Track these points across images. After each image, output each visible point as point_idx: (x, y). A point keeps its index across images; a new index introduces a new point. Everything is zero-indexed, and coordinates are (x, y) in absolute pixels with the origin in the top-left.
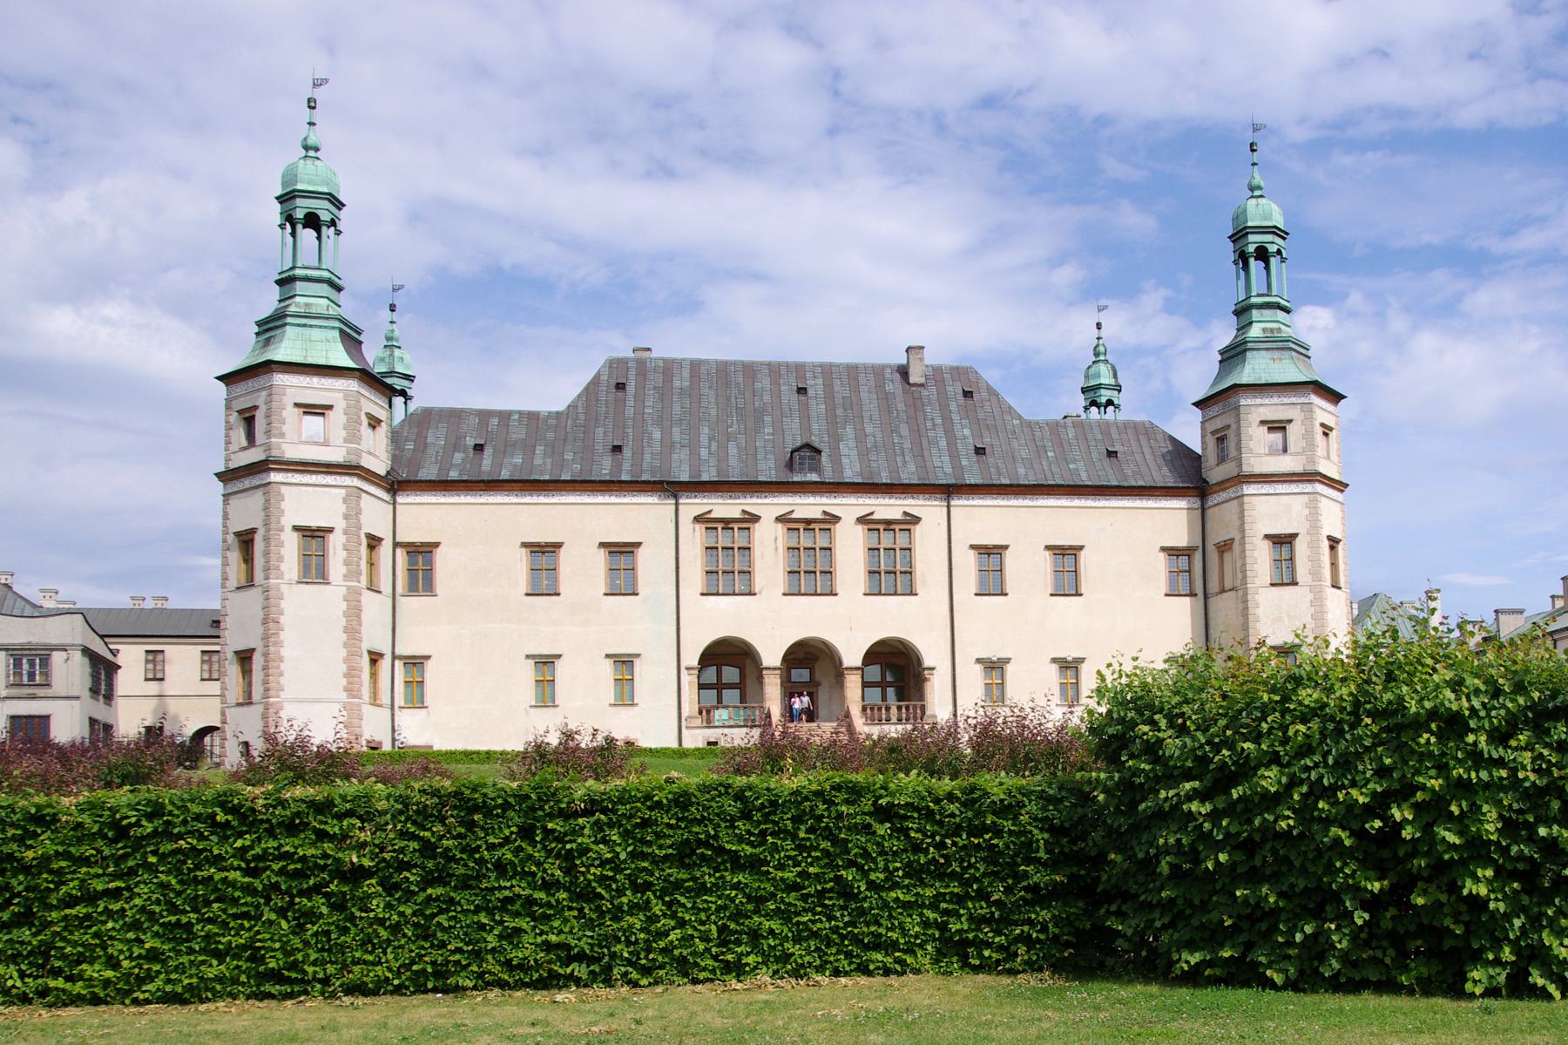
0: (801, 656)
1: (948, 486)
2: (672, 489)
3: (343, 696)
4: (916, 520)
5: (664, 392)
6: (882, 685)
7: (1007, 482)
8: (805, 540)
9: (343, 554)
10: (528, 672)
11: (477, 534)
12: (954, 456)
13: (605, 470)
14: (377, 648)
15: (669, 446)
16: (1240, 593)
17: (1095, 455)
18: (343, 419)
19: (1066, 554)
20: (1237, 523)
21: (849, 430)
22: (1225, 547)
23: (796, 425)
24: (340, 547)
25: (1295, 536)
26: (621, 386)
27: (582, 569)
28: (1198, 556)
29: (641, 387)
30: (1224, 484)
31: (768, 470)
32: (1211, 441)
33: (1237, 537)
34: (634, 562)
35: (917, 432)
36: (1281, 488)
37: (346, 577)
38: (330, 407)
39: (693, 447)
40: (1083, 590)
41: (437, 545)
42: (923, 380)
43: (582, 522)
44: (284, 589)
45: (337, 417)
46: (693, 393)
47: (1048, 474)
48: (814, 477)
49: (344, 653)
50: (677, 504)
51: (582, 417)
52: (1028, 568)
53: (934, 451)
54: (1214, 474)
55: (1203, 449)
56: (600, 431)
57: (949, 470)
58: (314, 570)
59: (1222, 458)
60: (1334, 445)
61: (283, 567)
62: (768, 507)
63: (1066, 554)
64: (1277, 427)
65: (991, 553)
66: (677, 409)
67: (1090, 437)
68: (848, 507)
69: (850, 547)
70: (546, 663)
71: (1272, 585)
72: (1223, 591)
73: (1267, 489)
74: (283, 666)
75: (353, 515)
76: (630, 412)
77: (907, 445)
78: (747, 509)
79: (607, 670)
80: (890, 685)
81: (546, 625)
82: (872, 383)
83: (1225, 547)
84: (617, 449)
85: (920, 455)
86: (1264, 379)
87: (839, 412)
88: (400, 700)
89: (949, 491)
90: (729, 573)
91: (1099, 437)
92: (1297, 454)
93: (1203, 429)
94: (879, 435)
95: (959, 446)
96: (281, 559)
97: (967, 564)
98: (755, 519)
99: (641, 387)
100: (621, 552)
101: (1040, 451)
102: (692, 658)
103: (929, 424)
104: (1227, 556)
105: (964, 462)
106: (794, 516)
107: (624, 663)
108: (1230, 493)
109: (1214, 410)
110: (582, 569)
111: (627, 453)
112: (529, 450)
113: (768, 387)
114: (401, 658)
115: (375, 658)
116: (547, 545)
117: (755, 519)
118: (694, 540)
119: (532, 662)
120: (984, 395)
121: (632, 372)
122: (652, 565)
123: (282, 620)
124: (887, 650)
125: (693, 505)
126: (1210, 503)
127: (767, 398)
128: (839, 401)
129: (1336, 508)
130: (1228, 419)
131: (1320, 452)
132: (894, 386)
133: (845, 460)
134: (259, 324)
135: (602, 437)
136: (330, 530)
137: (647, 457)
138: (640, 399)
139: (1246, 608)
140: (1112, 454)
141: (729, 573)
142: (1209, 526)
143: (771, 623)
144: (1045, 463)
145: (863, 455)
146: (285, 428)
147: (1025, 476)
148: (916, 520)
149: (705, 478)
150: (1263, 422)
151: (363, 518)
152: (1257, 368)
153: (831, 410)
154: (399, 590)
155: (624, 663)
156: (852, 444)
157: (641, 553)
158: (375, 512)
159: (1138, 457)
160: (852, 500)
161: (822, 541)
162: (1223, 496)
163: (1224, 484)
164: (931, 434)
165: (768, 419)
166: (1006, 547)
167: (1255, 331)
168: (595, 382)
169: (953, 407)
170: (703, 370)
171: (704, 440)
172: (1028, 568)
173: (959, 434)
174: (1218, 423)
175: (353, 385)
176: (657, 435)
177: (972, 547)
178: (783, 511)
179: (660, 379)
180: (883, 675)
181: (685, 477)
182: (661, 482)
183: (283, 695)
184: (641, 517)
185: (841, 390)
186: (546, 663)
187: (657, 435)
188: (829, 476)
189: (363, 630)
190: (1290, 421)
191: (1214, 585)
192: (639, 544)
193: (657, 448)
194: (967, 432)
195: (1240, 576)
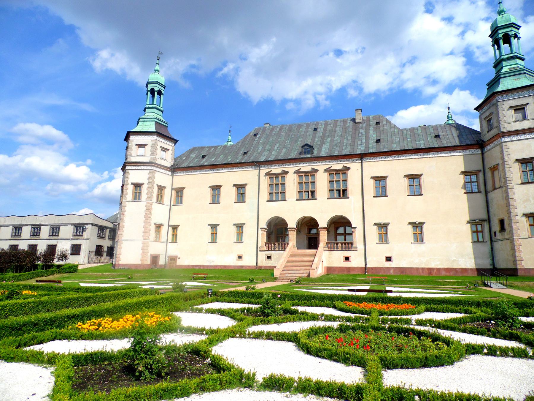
1: (361, 154)
2: (258, 164)
3: (142, 239)
4: (348, 169)
7: (387, 150)
8: (304, 180)
9: (146, 191)
10: (209, 230)
11: (197, 183)
12: (367, 143)
14: (160, 222)
15: (263, 151)
16: (504, 189)
17: (429, 138)
19: (414, 179)
20: (500, 156)
21: (329, 140)
22: (494, 169)
24: (146, 189)
26: (255, 135)
27: (228, 194)
28: (481, 175)
31: (293, 155)
32: (485, 123)
33: (500, 162)
34: (244, 191)
35: (354, 138)
36: (523, 137)
37: (147, 199)
38: (146, 145)
39: (271, 151)
40: (423, 193)
41: (184, 188)
42: (361, 121)
43: (228, 178)
44: (127, 203)
45: (148, 148)
47: (406, 146)
48: (309, 156)
49: (143, 224)
52: (397, 185)
54: (487, 137)
55: (481, 127)
56: (243, 149)
57: (363, 148)
58: (137, 197)
61: (127, 196)
62: (291, 169)
63: (414, 179)
64: (520, 109)
65: (380, 180)
66: (271, 140)
68: (321, 167)
69: (322, 182)
70: (214, 227)
71: (522, 183)
72: (495, 189)
74: (124, 229)
75: (151, 179)
76: (255, 142)
78: (284, 169)
79: (234, 229)
83: (494, 169)
84: (245, 153)
85: (353, 143)
86: (510, 87)
87: (327, 134)
88: (170, 239)
89: (362, 156)
90: (277, 193)
93: (481, 119)
95: (370, 140)
96: (127, 194)
97: (370, 185)
100: (240, 188)
101: (404, 138)
102: (263, 224)
103: (360, 135)
104: (496, 173)
105: (370, 146)
106: (301, 170)
107: (240, 227)
108: (496, 143)
109: (486, 108)
110: (228, 194)
111: (248, 154)
112: (219, 155)
114: (171, 226)
115: (159, 227)
116: (217, 186)
117: (287, 173)
118: (265, 182)
120: (385, 123)
121: (261, 131)
122: (250, 192)
123: (125, 213)
124: (343, 221)
126: (486, 150)
130: (493, 110)
132: (350, 124)
133: (323, 150)
135: (243, 150)
136: (143, 184)
137: (254, 155)
138: (260, 139)
139: (507, 196)
141: (277, 193)
142: (486, 160)
143: (292, 211)
144: (405, 143)
146: (132, 152)
147: (395, 147)
148: (348, 169)
150: (511, 107)
151: (155, 180)
152: (505, 84)
153: (324, 134)
154: (172, 204)
155: (240, 227)
156: (328, 144)
157: (247, 188)
158: (163, 178)
159: (450, 136)
161: (310, 179)
162: (492, 145)
165: (300, 139)
166: (387, 177)
167: (505, 69)
168: (249, 135)
169: (371, 128)
171: (275, 148)
172: (397, 185)
173: (371, 136)
174: (487, 113)
175: (155, 137)
176: (261, 148)
177: (372, 178)
182: (253, 162)
183: (123, 238)
184: (248, 176)
186: (214, 227)
187: (261, 148)
188: (315, 154)
189: (152, 217)
190: (527, 104)
191: (490, 186)
192: (246, 185)
193: (259, 152)
194: (374, 135)
195: (503, 180)
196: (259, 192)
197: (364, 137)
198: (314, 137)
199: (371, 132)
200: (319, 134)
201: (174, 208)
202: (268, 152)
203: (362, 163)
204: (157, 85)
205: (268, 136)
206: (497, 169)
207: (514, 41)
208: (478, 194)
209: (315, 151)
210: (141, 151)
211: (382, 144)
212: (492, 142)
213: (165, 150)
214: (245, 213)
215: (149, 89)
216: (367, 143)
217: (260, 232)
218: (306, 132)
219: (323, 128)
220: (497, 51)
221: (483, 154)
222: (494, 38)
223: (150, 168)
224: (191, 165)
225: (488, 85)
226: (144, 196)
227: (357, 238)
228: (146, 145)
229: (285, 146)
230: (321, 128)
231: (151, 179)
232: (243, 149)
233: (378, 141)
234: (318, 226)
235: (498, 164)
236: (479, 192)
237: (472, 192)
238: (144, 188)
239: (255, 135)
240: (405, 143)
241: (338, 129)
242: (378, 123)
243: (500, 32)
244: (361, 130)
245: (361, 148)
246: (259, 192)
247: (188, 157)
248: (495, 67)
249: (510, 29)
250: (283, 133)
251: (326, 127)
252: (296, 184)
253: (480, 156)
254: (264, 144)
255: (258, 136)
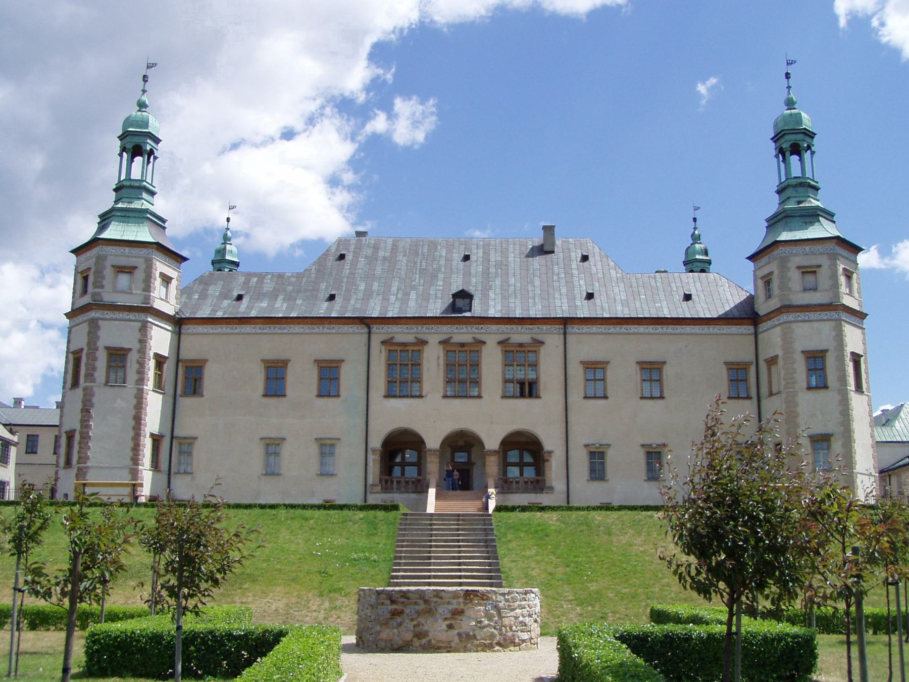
0: (461, 443)
5: (372, 260)
6: (521, 465)
12: (571, 299)
13: (322, 309)
15: (368, 295)
18: (143, 276)
19: (652, 370)
21: (498, 282)
23: (460, 280)
25: (827, 351)
26: (342, 257)
27: (302, 380)
28: (753, 369)
29: (356, 255)
30: (770, 315)
32: (760, 284)
36: (813, 315)
40: (665, 395)
46: (391, 260)
47: (640, 311)
48: (467, 314)
50: (369, 333)
51: (313, 276)
53: (557, 296)
54: (763, 308)
59: (769, 296)
60: (855, 286)
62: (434, 336)
63: (652, 370)
64: (808, 271)
65: (595, 369)
66: (378, 271)
67: (673, 285)
68: (492, 336)
69: (492, 364)
72: (771, 394)
73: (802, 316)
77: (538, 291)
78: (418, 336)
80: (529, 465)
81: (276, 418)
82: (517, 251)
83: (772, 361)
84: (332, 298)
87: (492, 270)
91: (679, 284)
92: (826, 290)
93: (755, 275)
94: (518, 284)
98: (425, 343)
99: (356, 255)
102: (376, 442)
103: (555, 278)
104: (773, 369)
105: (578, 303)
108: (775, 321)
109: (764, 260)
110: (302, 380)
112: (274, 296)
113: (444, 254)
117: (425, 343)
119: (263, 442)
122: (350, 378)
124: (523, 439)
125: (380, 333)
126: (760, 330)
127: (442, 262)
128: (492, 263)
129: (858, 332)
131: (843, 289)
134: (100, 216)
135: (324, 289)
137: (352, 302)
138: (354, 263)
140: (688, 297)
143: (434, 417)
145: (505, 298)
149: (390, 315)
150: (799, 268)
154: (179, 392)
156: (498, 291)
160: (494, 328)
163: (770, 315)
164: (556, 284)
165: (441, 276)
169: (574, 266)
170: (401, 244)
171: (394, 289)
173: (576, 283)
174: (765, 271)
178: (444, 337)
179: (369, 252)
180: (521, 457)
181: (375, 314)
185: (494, 257)
187: (362, 287)
190: (819, 266)
191: (764, 390)
193: (361, 295)
194: (582, 282)
196: (368, 378)
197: (563, 282)
198: (467, 274)
199: (575, 272)
200: (476, 266)
201: (186, 403)
202: (381, 297)
203: (565, 334)
204: (149, 141)
205: (372, 260)
206: (776, 363)
207: (807, 155)
208: (747, 402)
209: (476, 304)
210: (124, 279)
211: (597, 299)
212: (770, 319)
213: (166, 280)
214: (338, 418)
215: (129, 146)
216: (571, 299)
217: (371, 457)
218: (449, 260)
219: (481, 254)
220: (782, 165)
221: (756, 334)
222: (778, 144)
223: (142, 316)
224: (219, 314)
225: (768, 220)
226: (132, 376)
227: (554, 471)
228: (135, 268)
229: (413, 288)
230: (477, 255)
231: (143, 341)
232: (323, 286)
233: (590, 296)
234: (484, 448)
235: (777, 356)
236: (749, 398)
237: (738, 398)
238: (133, 357)
239: (342, 257)
240: (638, 305)
241: (511, 259)
242: (585, 258)
243: (787, 137)
244: (556, 268)
245: (562, 309)
246: (368, 378)
247: (204, 296)
248: (779, 192)
249: (801, 137)
250: (403, 260)
251: (486, 254)
252: (442, 367)
253: (753, 337)
254: (369, 277)
255: (349, 257)
